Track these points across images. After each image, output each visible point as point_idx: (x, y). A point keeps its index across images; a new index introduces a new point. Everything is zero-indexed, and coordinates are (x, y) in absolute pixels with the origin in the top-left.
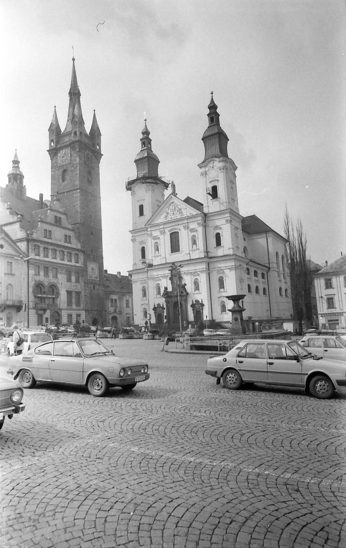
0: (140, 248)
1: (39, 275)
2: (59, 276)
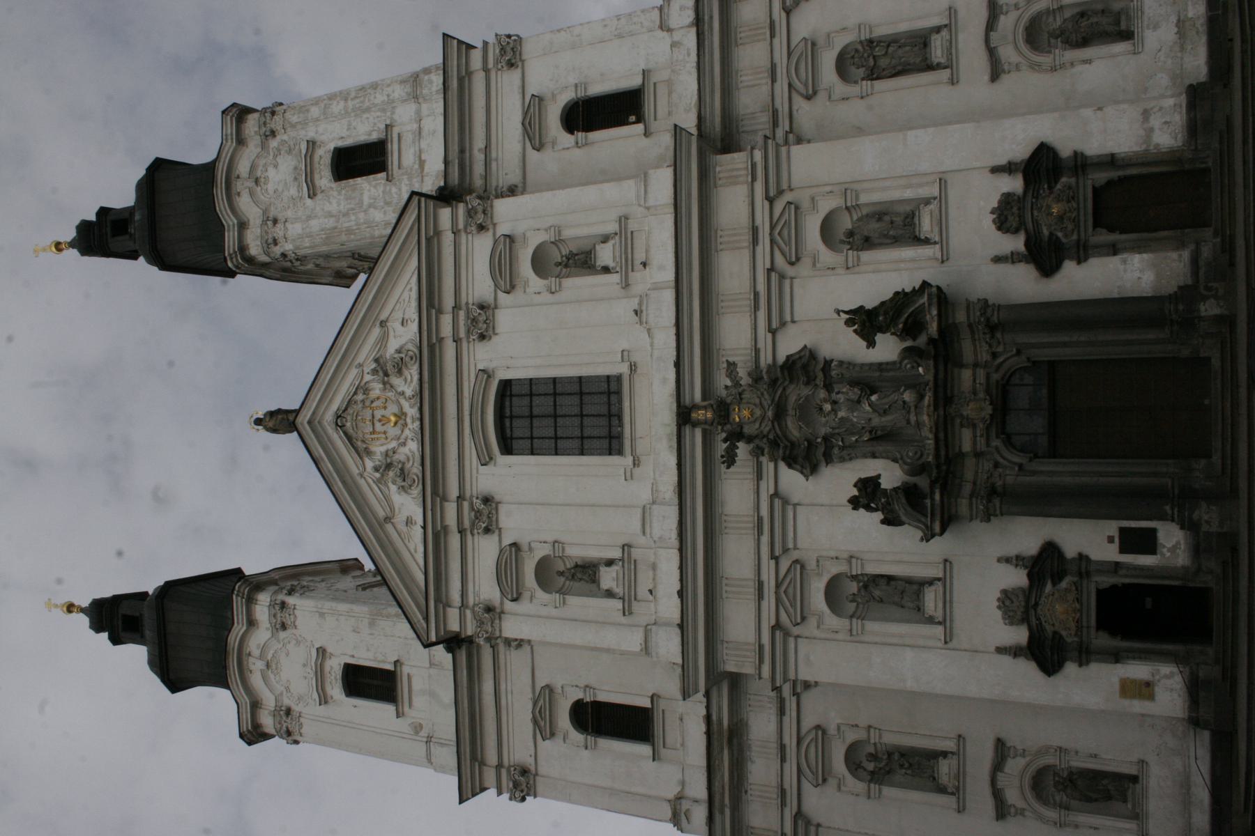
0: (577, 736)
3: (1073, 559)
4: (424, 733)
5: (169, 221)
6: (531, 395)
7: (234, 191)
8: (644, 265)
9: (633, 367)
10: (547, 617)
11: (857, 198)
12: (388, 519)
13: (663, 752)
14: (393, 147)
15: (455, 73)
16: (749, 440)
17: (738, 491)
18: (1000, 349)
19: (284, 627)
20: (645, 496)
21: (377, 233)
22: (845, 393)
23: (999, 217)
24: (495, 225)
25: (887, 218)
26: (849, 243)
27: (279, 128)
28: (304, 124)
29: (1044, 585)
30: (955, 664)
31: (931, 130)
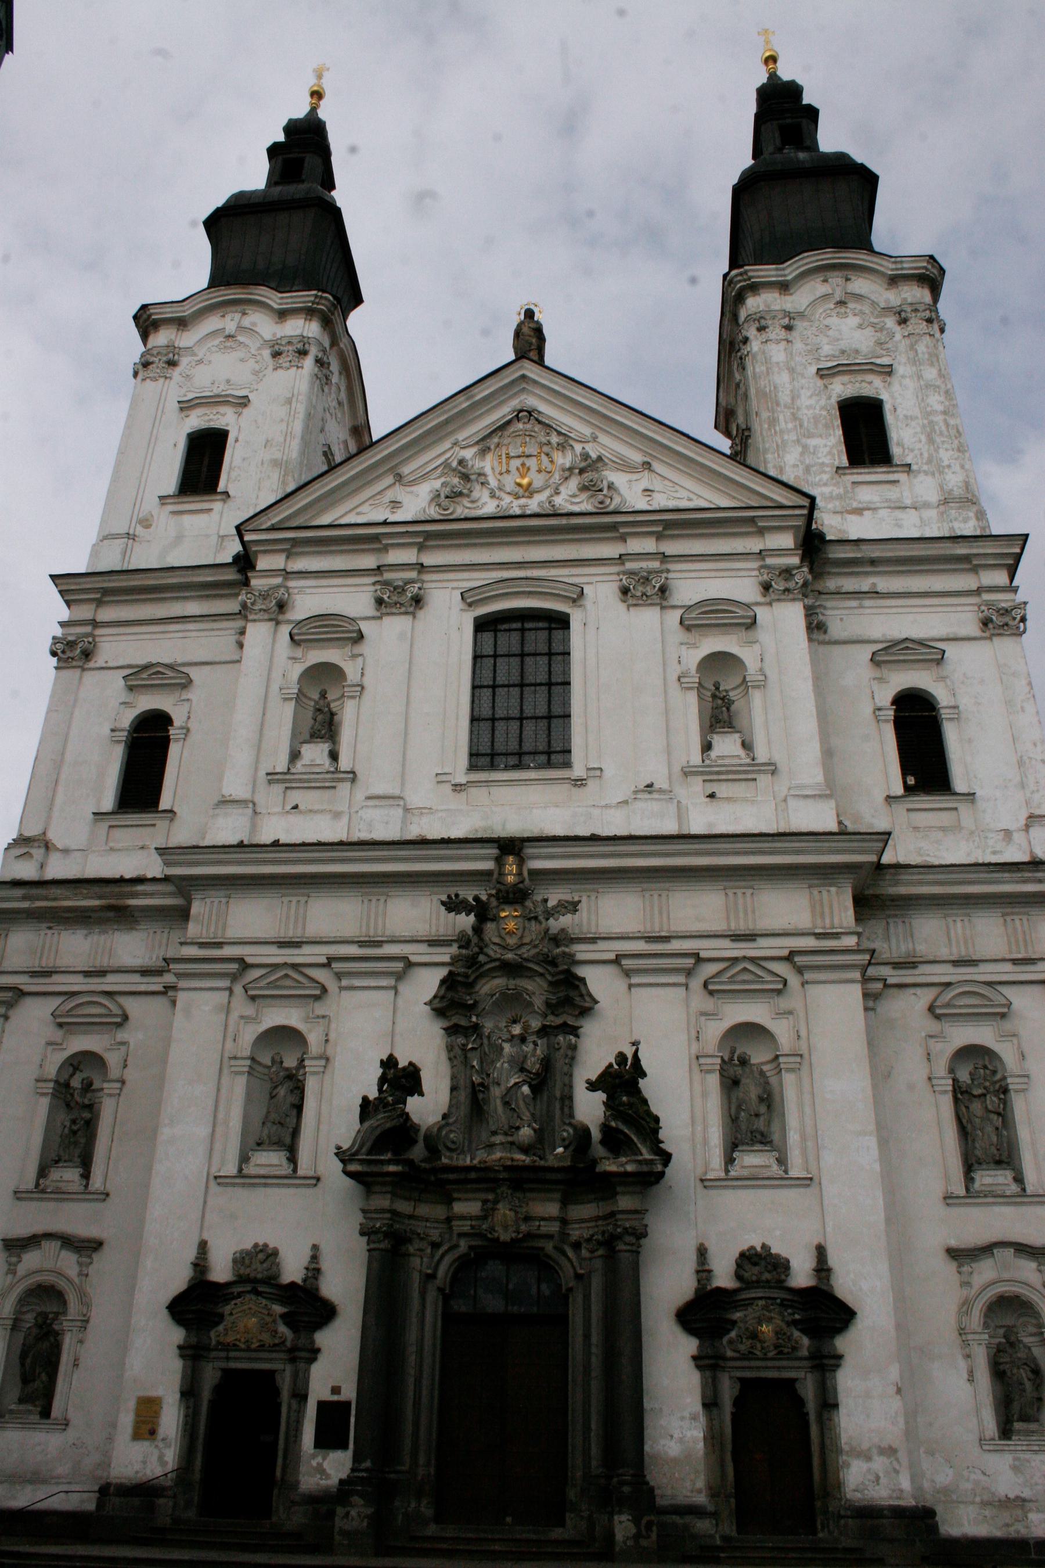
3: (313, 1342)
4: (140, 530)
5: (799, 195)
6: (550, 654)
7: (828, 274)
8: (712, 796)
9: (579, 783)
10: (268, 679)
11: (788, 1070)
12: (399, 478)
13: (105, 825)
14: (878, 474)
15: (975, 551)
16: (478, 930)
17: (414, 916)
18: (584, 1253)
19: (276, 355)
20: (415, 799)
21: (769, 456)
22: (535, 1052)
23: (757, 1255)
24: (770, 604)
25: (763, 1109)
26: (731, 1059)
27: (910, 328)
28: (915, 362)
29: (283, 1303)
30: (192, 1191)
31: (877, 1167)
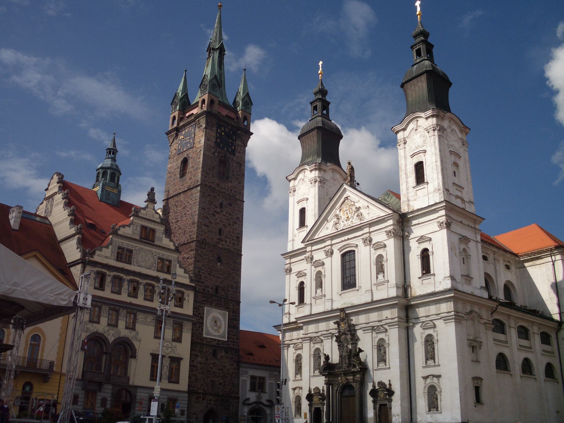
0: (298, 283)
1: (98, 322)
2: (138, 326)
9: (358, 290)
17: (332, 325)
